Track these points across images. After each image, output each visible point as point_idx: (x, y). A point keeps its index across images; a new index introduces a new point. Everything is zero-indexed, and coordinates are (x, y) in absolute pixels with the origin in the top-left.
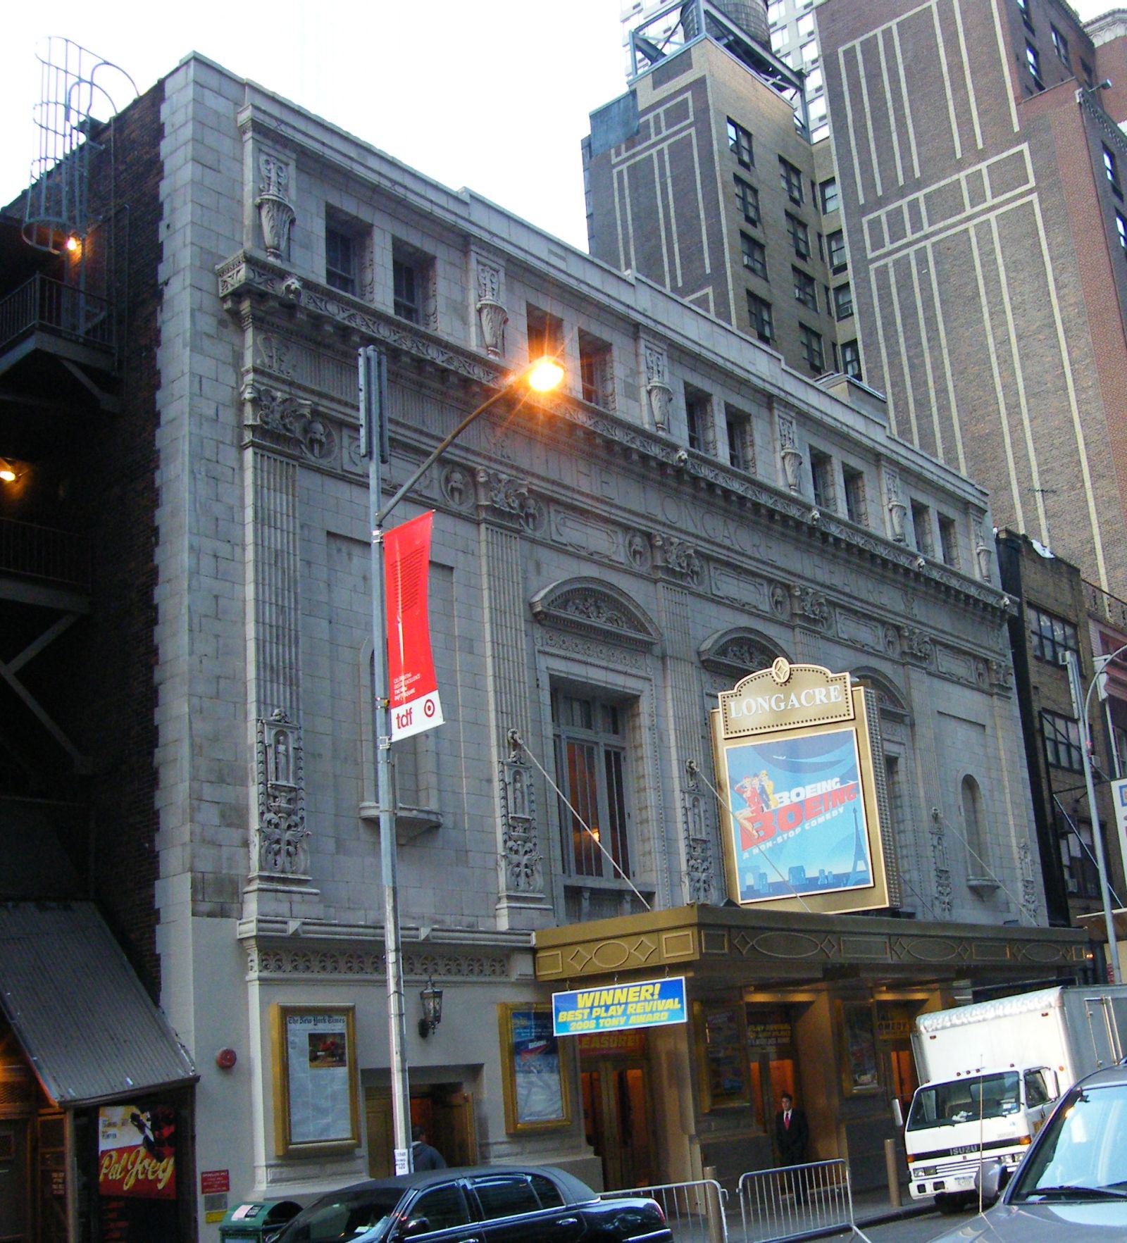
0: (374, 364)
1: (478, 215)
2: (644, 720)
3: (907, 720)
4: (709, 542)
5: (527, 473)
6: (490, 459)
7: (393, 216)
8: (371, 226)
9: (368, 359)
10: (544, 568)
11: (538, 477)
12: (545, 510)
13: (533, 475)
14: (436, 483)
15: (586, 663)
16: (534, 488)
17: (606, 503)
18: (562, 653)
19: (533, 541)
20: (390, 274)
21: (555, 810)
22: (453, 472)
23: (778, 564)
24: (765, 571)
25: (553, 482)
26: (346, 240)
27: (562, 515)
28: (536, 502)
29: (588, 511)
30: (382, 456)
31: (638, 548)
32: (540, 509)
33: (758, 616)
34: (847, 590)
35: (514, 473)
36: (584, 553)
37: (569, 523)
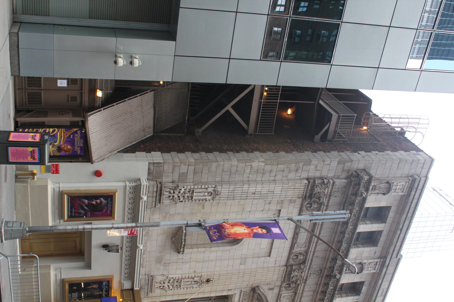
0: (344, 216)
1: (394, 260)
5: (305, 283)
6: (309, 269)
7: (389, 231)
8: (385, 223)
9: (345, 214)
10: (271, 291)
11: (304, 288)
12: (292, 291)
13: (304, 286)
14: (299, 249)
16: (300, 286)
19: (281, 287)
20: (370, 230)
21: (184, 298)
22: (303, 255)
25: (302, 294)
26: (379, 214)
27: (290, 298)
28: (294, 288)
30: (312, 220)
32: (292, 289)
35: (305, 278)
37: (288, 300)
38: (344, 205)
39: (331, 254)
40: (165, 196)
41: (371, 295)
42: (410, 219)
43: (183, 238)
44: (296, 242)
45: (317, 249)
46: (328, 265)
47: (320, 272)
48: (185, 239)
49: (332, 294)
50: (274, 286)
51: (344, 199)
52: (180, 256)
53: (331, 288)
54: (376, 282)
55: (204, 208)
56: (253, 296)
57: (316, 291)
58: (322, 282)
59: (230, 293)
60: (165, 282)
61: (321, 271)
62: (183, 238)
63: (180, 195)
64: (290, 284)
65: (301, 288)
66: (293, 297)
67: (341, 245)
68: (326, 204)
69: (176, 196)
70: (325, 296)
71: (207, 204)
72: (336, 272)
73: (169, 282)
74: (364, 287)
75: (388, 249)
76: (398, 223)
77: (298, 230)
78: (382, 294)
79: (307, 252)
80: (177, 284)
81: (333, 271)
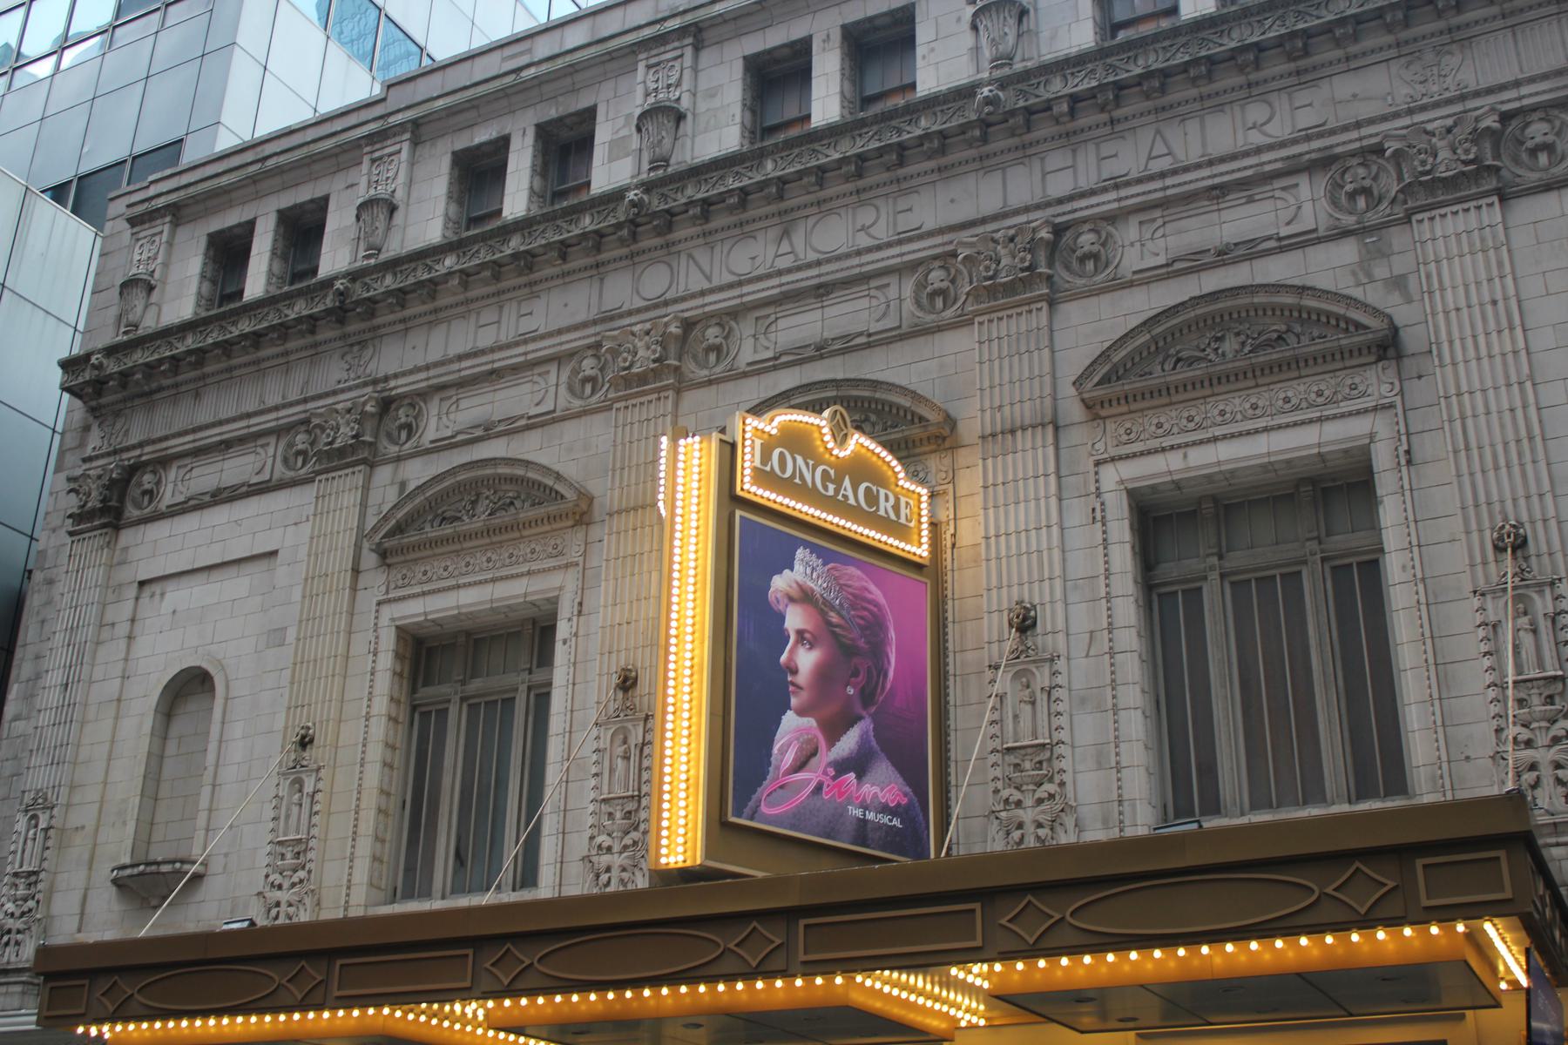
2: (563, 630)
3: (1412, 340)
4: (731, 286)
5: (386, 379)
6: (334, 393)
11: (404, 374)
13: (396, 376)
15: (458, 587)
17: (517, 344)
18: (417, 590)
19: (398, 459)
23: (930, 225)
24: (891, 257)
25: (427, 368)
29: (492, 372)
31: (589, 372)
33: (869, 346)
34: (1157, 166)
36: (479, 433)
37: (464, 404)
38: (152, 393)
39: (291, 345)
40: (13, 958)
41: (507, 96)
42: (259, 149)
43: (128, 872)
44: (243, 485)
45: (278, 400)
46: (329, 334)
47: (356, 348)
48: (133, 866)
49: (413, 265)
50: (392, 483)
51: (137, 402)
52: (216, 866)
53: (389, 280)
54: (451, 112)
55: (83, 827)
56: (401, 550)
57: (432, 318)
58: (391, 317)
59: (388, 640)
60: (273, 901)
61: (352, 345)
62: (128, 872)
63: (17, 914)
64: (401, 427)
65: (401, 386)
66: (452, 392)
67: (244, 336)
68: (137, 452)
69: (19, 924)
70: (420, 284)
71: (74, 820)
72: (329, 302)
73: (280, 887)
74: (477, 141)
75: (336, 155)
76: (254, 180)
77: (207, 498)
78: (522, 53)
79: (278, 432)
80: (289, 855)
81: (328, 312)
